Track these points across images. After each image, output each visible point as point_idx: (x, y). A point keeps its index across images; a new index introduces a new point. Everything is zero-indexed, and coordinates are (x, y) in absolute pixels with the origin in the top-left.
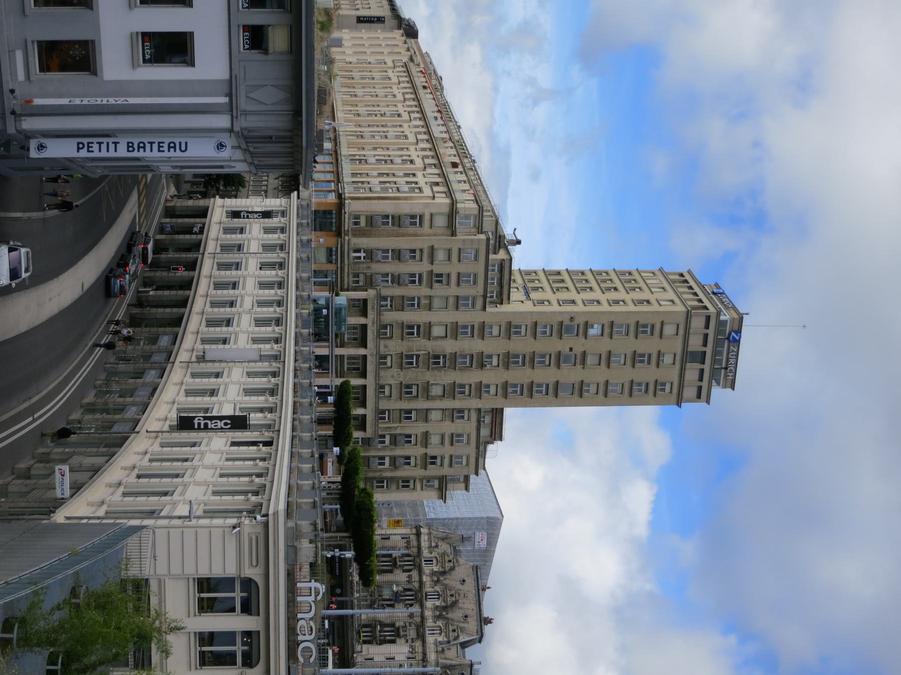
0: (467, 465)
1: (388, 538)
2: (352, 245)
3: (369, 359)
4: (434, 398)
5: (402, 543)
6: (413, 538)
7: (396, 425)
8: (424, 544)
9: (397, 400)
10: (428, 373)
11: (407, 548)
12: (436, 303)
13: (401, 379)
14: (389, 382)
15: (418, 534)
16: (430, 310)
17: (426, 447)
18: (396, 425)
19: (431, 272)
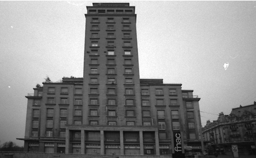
0: (175, 89)
1: (224, 133)
2: (43, 136)
3: (105, 130)
4: (134, 103)
5: (226, 129)
6: (223, 127)
7: (152, 119)
8: (226, 123)
9: (136, 119)
10: (119, 106)
11: (227, 128)
12: (78, 102)
13: (123, 117)
14: (125, 122)
15: (222, 125)
16: (82, 106)
17: (165, 106)
18: (152, 119)
19: (60, 105)
